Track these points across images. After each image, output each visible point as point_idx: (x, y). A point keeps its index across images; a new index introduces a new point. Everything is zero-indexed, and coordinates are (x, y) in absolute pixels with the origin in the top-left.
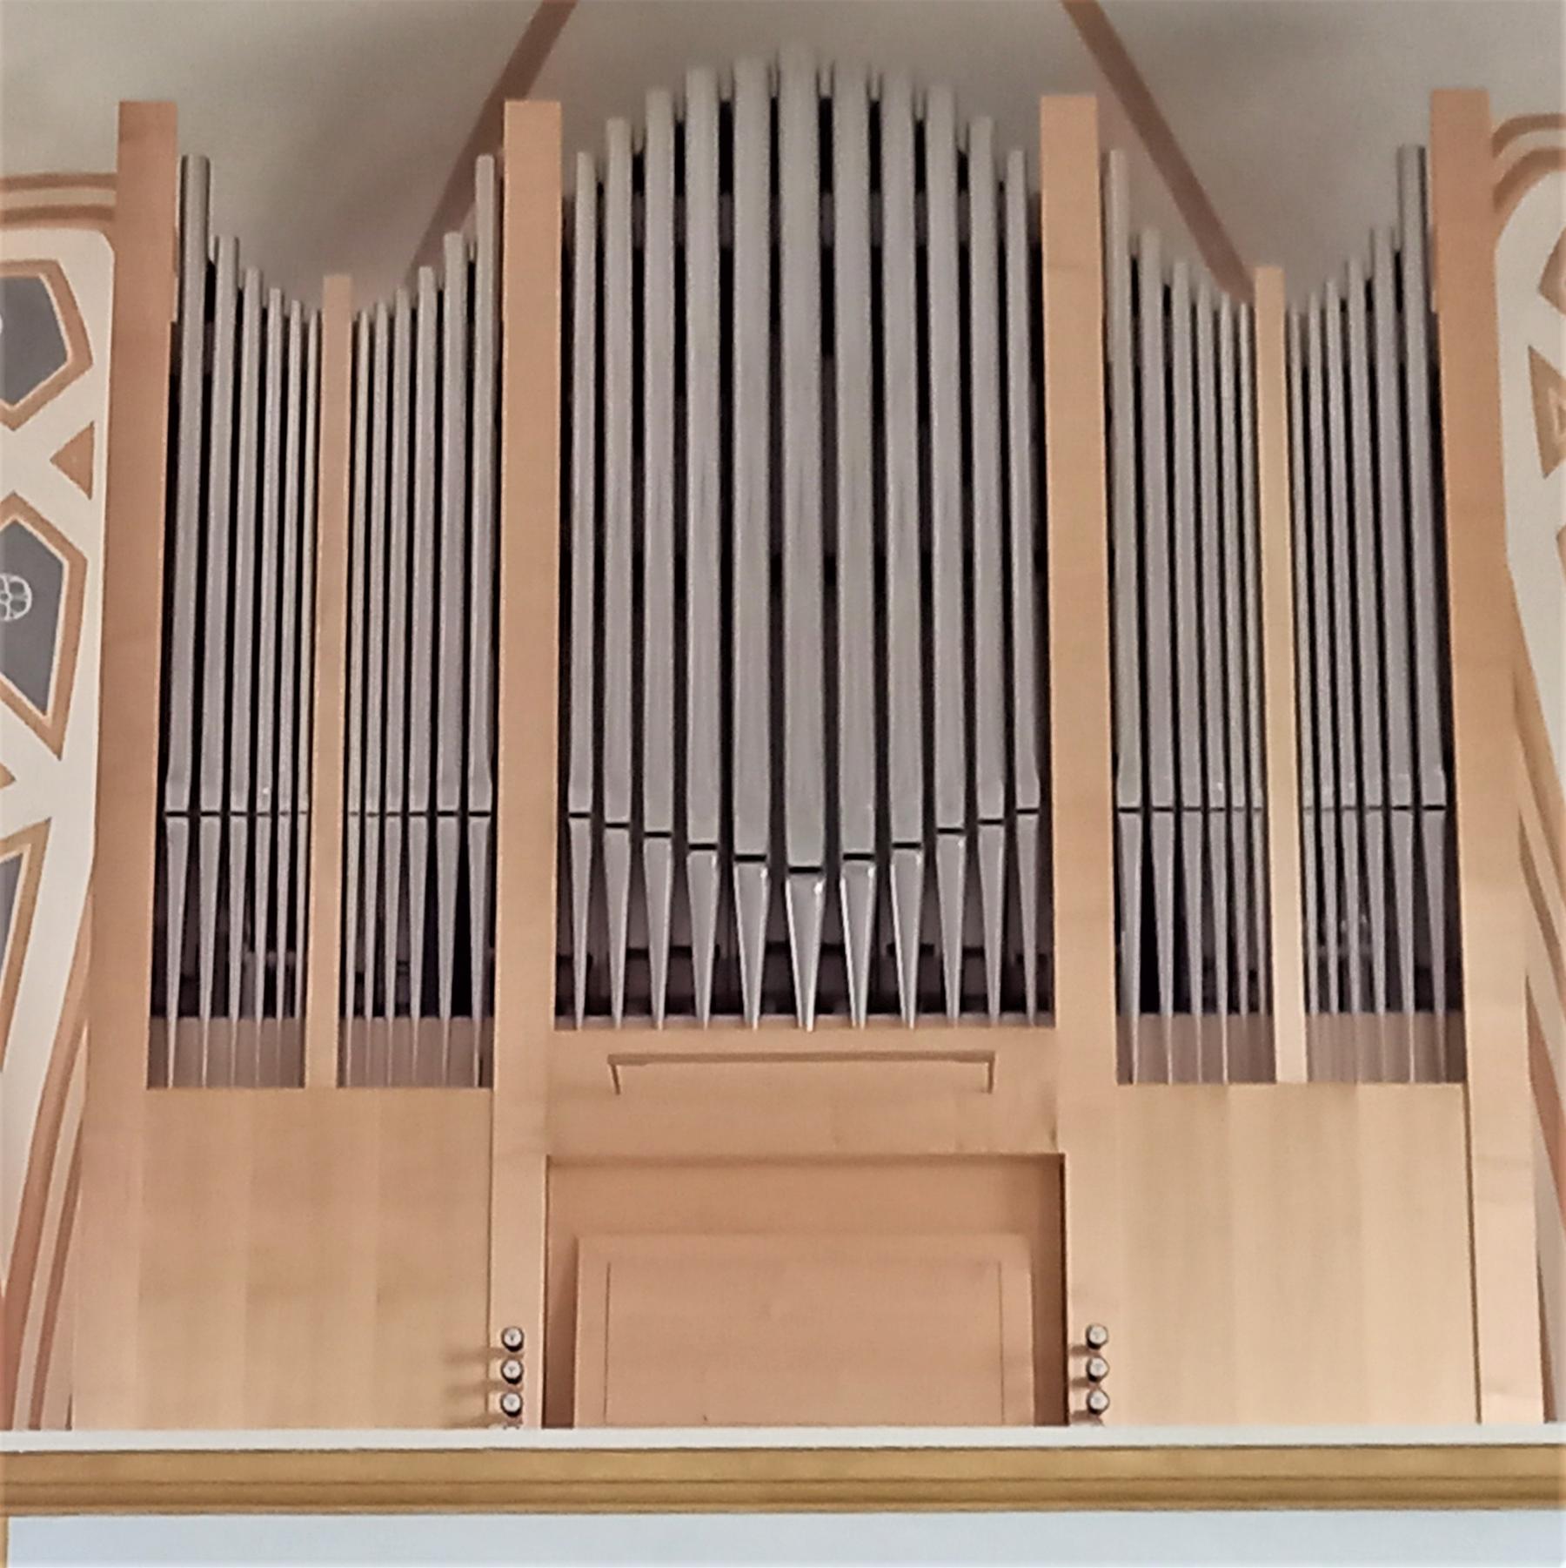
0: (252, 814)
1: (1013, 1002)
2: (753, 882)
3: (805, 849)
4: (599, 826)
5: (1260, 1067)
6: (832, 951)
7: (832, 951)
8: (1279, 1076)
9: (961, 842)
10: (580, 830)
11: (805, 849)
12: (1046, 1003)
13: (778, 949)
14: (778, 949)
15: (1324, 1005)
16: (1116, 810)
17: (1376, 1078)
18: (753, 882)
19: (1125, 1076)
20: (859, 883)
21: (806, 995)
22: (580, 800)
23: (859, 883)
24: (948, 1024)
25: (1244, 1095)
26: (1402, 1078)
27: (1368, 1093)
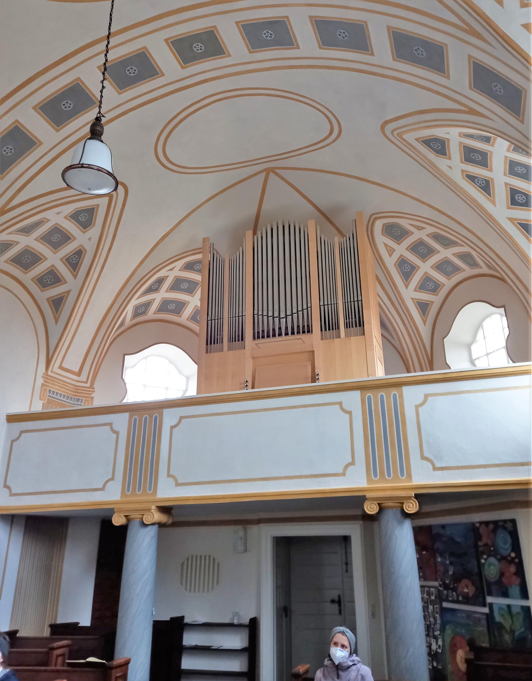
0: (218, 319)
1: (308, 332)
2: (277, 320)
3: (283, 315)
4: (258, 315)
5: (339, 336)
6: (287, 328)
7: (287, 328)
8: (341, 337)
9: (301, 312)
10: (256, 316)
11: (283, 315)
12: (312, 332)
13: (280, 328)
14: (280, 328)
15: (347, 328)
16: (320, 306)
17: (354, 336)
18: (277, 320)
19: (322, 339)
20: (289, 318)
21: (283, 333)
22: (256, 312)
23: (289, 318)
24: (301, 335)
25: (336, 340)
26: (358, 336)
27: (352, 338)
